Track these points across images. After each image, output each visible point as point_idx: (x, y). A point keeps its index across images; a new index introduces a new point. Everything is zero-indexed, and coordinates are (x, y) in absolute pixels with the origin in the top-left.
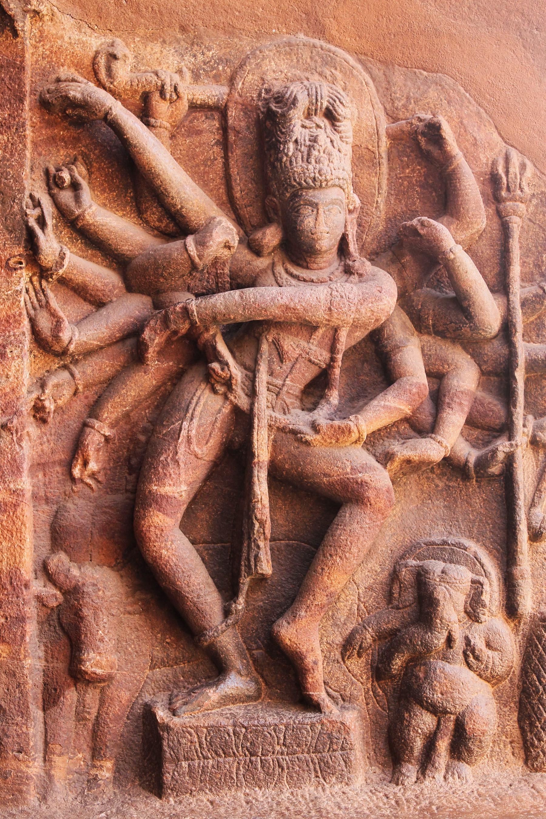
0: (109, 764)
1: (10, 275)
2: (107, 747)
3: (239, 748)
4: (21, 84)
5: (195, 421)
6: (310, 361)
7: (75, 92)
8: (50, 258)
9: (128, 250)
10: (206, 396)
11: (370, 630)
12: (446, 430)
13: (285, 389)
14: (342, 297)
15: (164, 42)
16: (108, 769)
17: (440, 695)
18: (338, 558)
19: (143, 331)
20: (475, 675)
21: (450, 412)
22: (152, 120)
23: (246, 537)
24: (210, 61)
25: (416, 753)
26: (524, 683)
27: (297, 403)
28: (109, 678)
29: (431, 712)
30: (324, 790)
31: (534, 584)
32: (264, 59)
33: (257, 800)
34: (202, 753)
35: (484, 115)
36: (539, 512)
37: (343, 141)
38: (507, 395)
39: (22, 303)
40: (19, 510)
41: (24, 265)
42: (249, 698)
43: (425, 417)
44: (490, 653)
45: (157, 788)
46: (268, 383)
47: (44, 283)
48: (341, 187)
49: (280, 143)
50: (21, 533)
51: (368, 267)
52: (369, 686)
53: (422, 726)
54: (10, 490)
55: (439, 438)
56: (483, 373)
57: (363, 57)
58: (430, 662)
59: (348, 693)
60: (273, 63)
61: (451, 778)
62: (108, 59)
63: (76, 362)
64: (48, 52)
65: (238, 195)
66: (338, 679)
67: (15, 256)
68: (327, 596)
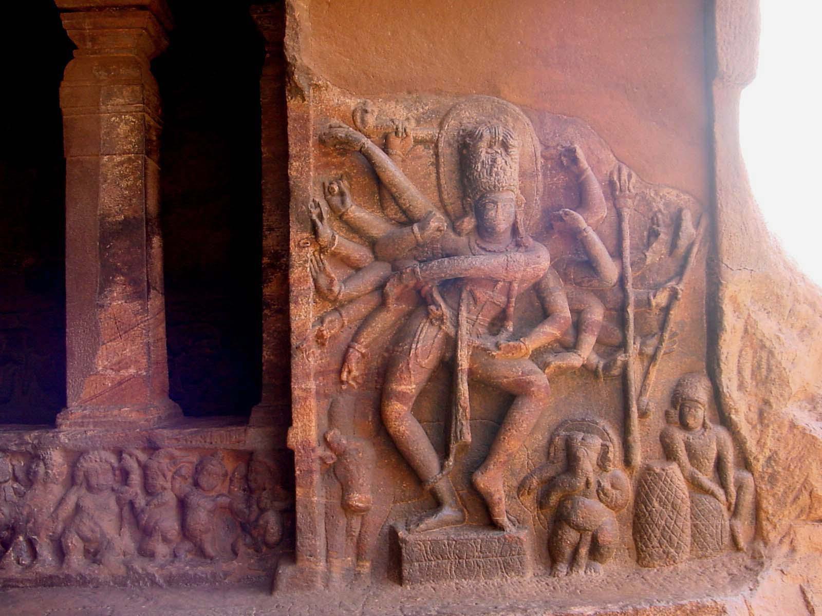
0: (368, 564)
4: (307, 130)
7: (341, 134)
9: (376, 234)
10: (427, 327)
13: (478, 321)
14: (514, 261)
15: (397, 101)
18: (515, 433)
19: (386, 285)
20: (604, 506)
23: (454, 417)
24: (427, 113)
28: (366, 509)
29: (576, 530)
30: (506, 580)
32: (461, 110)
35: (604, 143)
36: (645, 399)
39: (308, 269)
40: (308, 402)
41: (309, 245)
42: (457, 522)
43: (570, 339)
44: (614, 491)
45: (399, 579)
48: (512, 191)
50: (309, 416)
52: (536, 513)
53: (570, 539)
54: (302, 389)
56: (607, 309)
57: (525, 108)
60: (467, 113)
61: (589, 573)
62: (362, 113)
63: (342, 306)
65: (446, 197)
67: (303, 239)
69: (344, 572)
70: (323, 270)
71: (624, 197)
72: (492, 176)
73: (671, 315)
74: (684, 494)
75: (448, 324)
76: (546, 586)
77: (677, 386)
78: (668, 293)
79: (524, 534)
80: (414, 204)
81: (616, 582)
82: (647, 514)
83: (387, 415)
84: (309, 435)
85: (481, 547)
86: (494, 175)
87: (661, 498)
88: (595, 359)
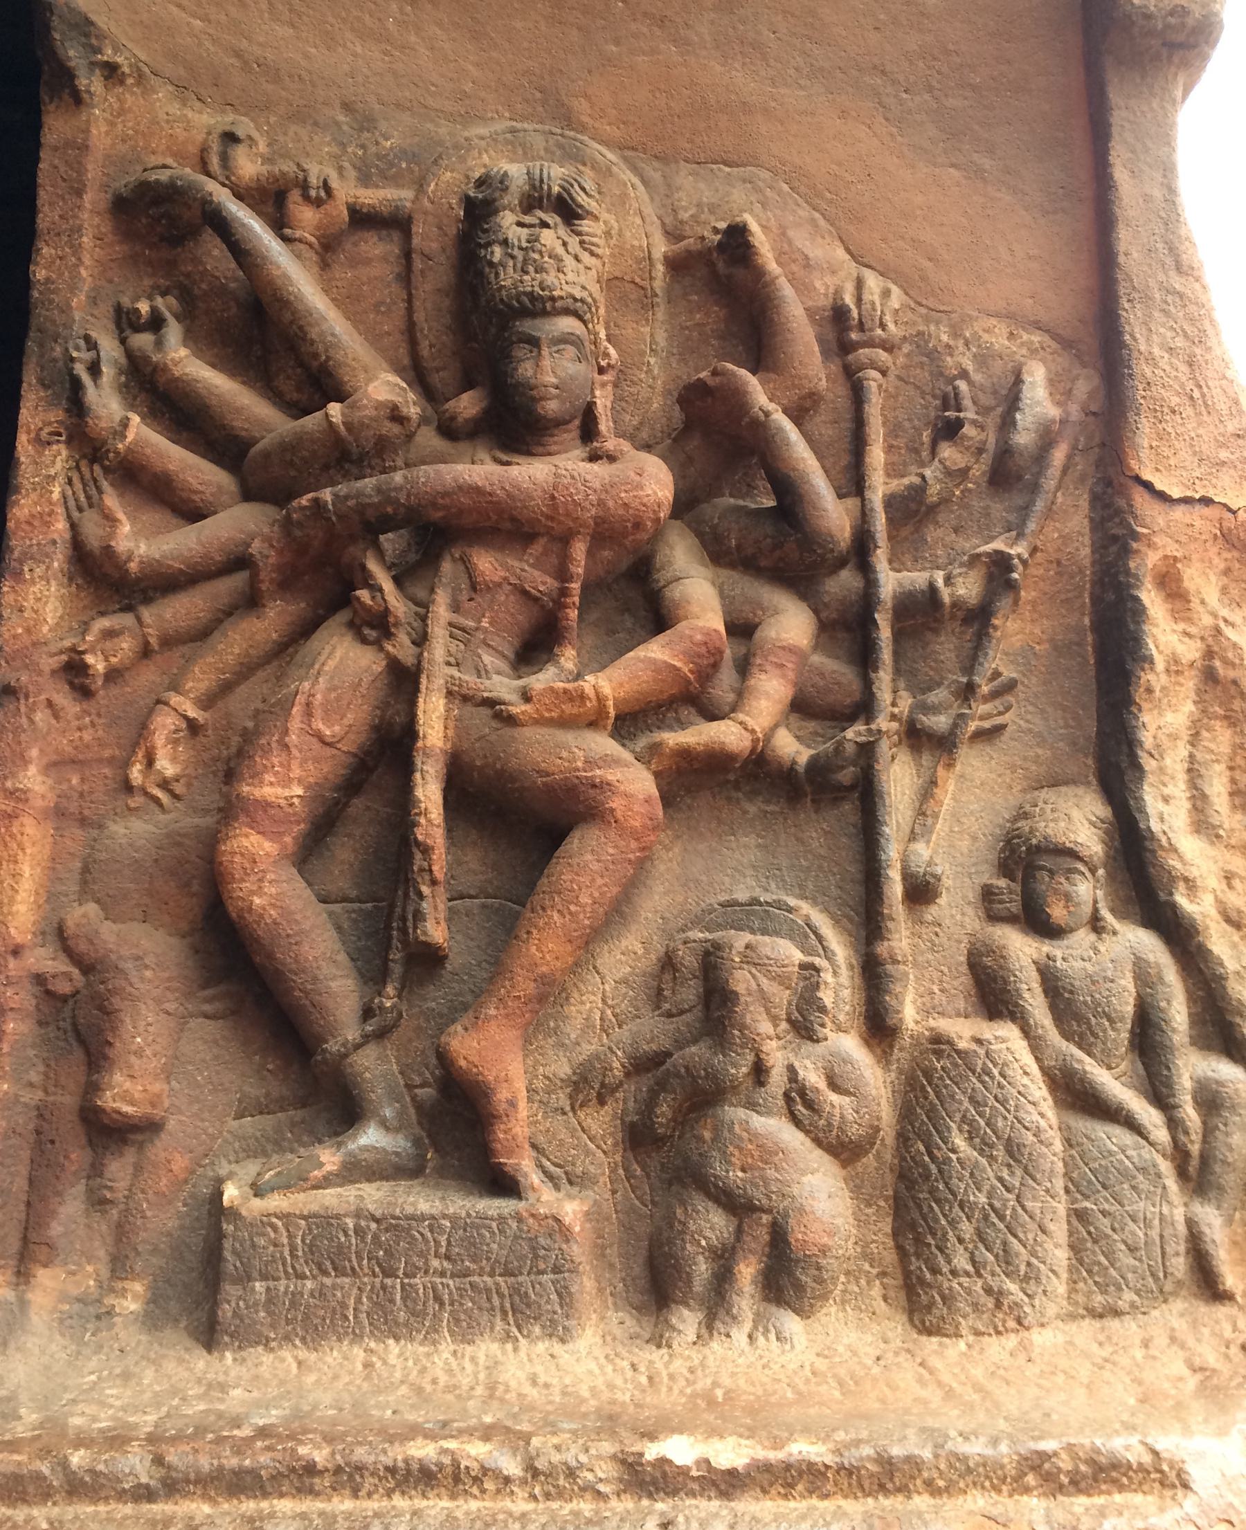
1: (41, 454)
2: (138, 1254)
4: (80, 169)
6: (525, 593)
7: (163, 176)
8: (103, 424)
14: (573, 477)
15: (316, 124)
16: (136, 1297)
17: (740, 1174)
18: (556, 916)
21: (763, 677)
22: (287, 231)
27: (504, 666)
28: (150, 1127)
30: (516, 1349)
33: (385, 1363)
34: (293, 1267)
35: (822, 222)
36: (922, 851)
39: (56, 495)
44: (834, 1097)
45: (209, 1335)
47: (96, 468)
49: (480, 246)
51: (626, 446)
52: (618, 1158)
53: (708, 1233)
55: (741, 716)
59: (579, 1170)
63: (148, 601)
66: (562, 1143)
71: (871, 344)
73: (995, 628)
74: (1042, 1115)
75: (403, 638)
76: (629, 1373)
77: (1015, 819)
78: (984, 570)
79: (572, 1209)
80: (339, 356)
81: (842, 1372)
82: (933, 1167)
83: (221, 863)
84: (10, 913)
86: (531, 269)
87: (971, 1123)
88: (792, 747)
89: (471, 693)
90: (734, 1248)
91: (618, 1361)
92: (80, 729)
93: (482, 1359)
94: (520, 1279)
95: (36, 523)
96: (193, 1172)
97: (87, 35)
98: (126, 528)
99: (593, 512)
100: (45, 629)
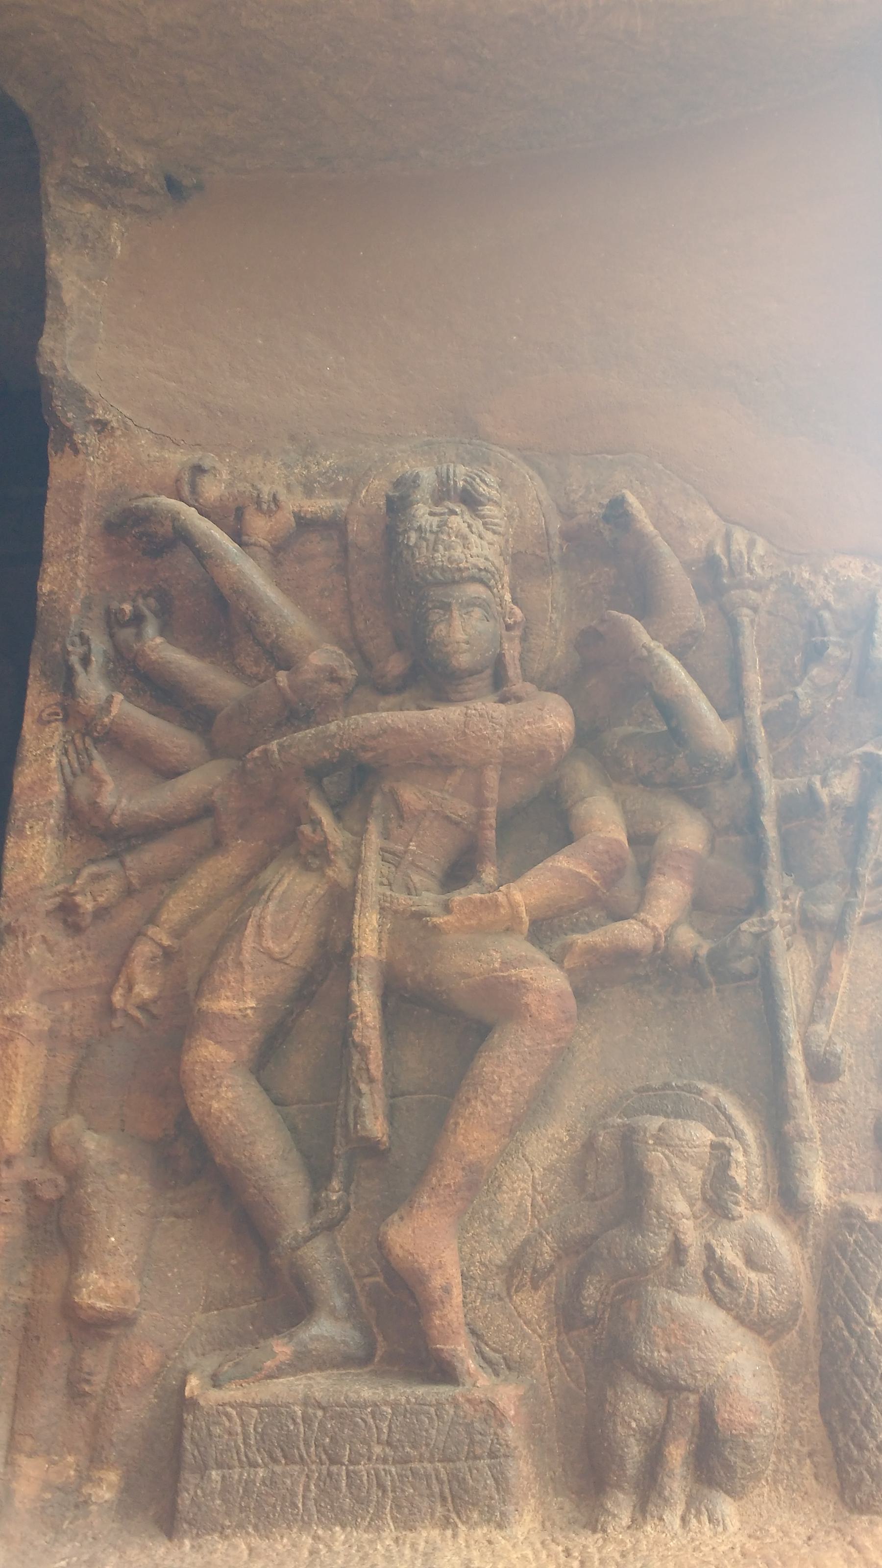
2: (112, 1444)
3: (310, 1447)
5: (272, 906)
6: (447, 818)
8: (92, 703)
11: (549, 1238)
12: (654, 903)
14: (481, 716)
16: (110, 1486)
17: (664, 1354)
18: (479, 1106)
21: (662, 879)
25: (631, 1470)
26: (825, 1334)
30: (455, 1536)
31: (827, 1155)
33: (330, 1549)
37: (488, 529)
38: (755, 854)
39: (54, 763)
44: (753, 1275)
45: (169, 1524)
46: (382, 849)
47: (88, 740)
50: (10, 1081)
51: (530, 688)
52: (553, 1341)
53: (637, 1415)
58: (647, 1291)
60: (407, 466)
61: (694, 1521)
63: (131, 849)
64: (119, 472)
65: (362, 626)
67: (50, 706)
68: (463, 1169)
69: (48, 1496)
70: (86, 769)
72: (437, 551)
85: (390, 1427)
89: (401, 908)
90: (664, 1429)
91: (553, 1546)
92: (72, 961)
93: (422, 1546)
94: (459, 1464)
95: (36, 788)
96: (163, 1365)
97: (82, 401)
98: (110, 786)
99: (501, 744)
100: (42, 876)
